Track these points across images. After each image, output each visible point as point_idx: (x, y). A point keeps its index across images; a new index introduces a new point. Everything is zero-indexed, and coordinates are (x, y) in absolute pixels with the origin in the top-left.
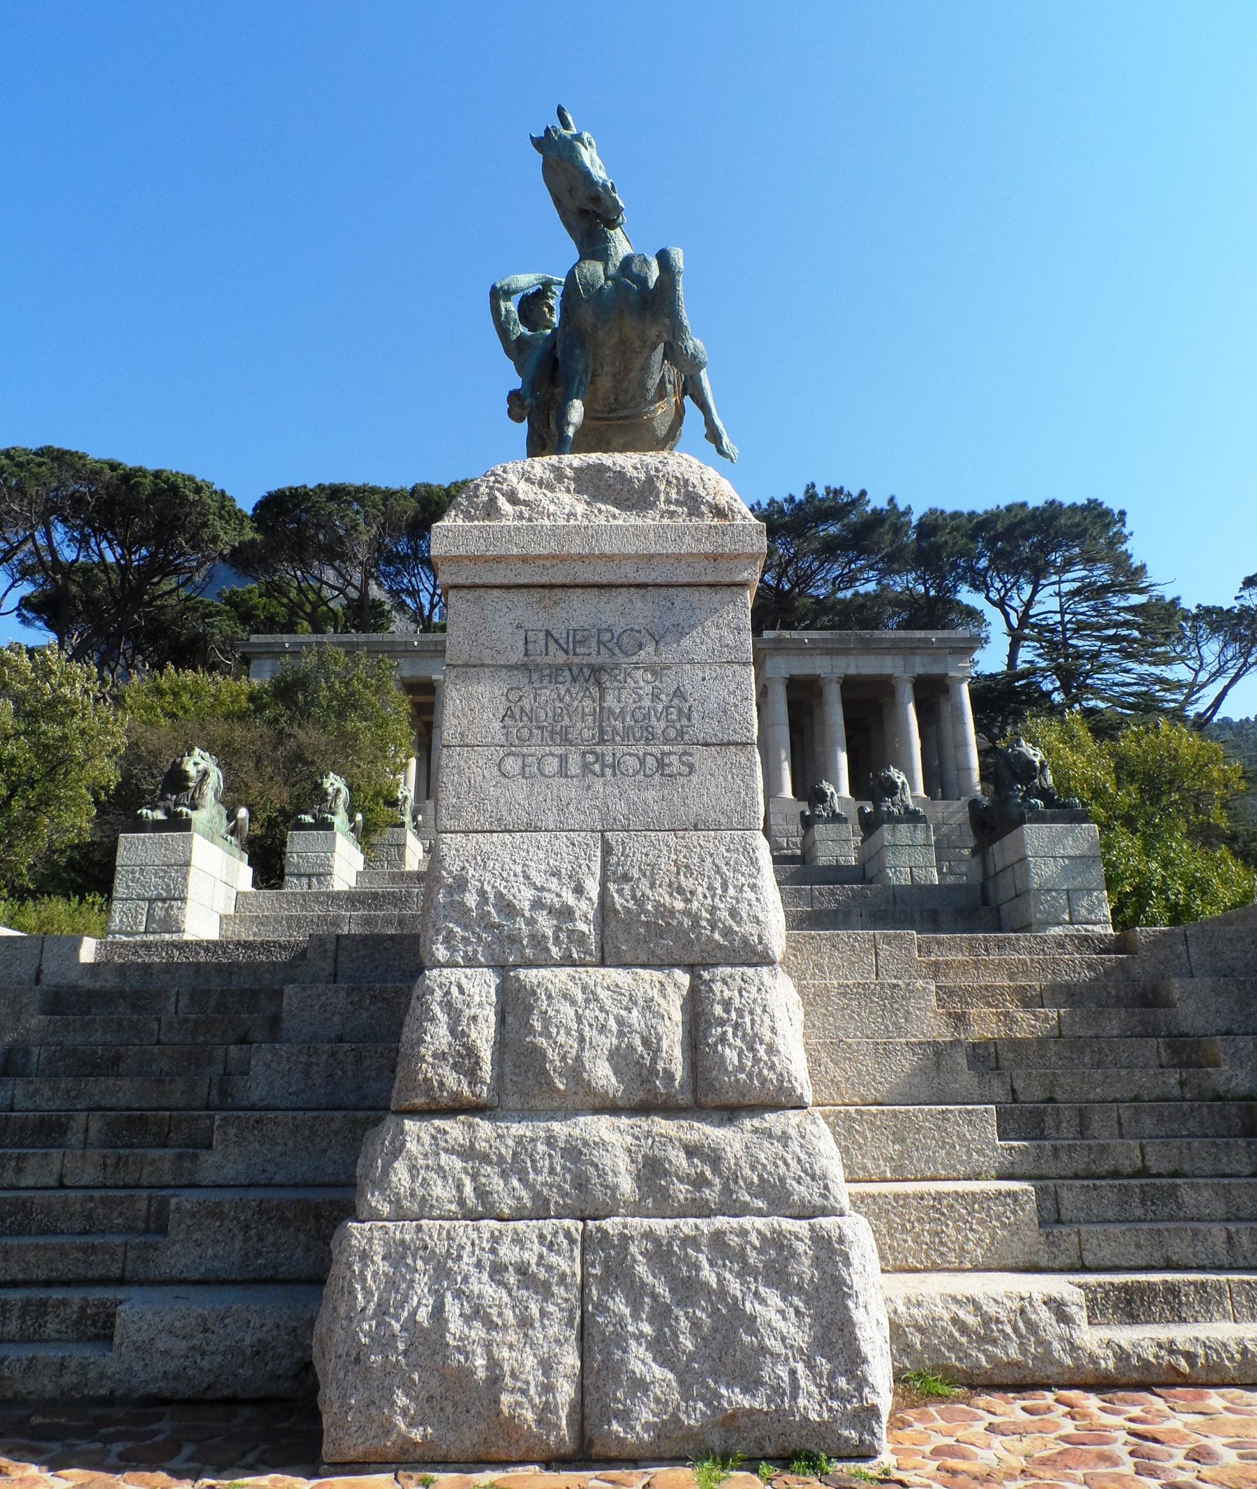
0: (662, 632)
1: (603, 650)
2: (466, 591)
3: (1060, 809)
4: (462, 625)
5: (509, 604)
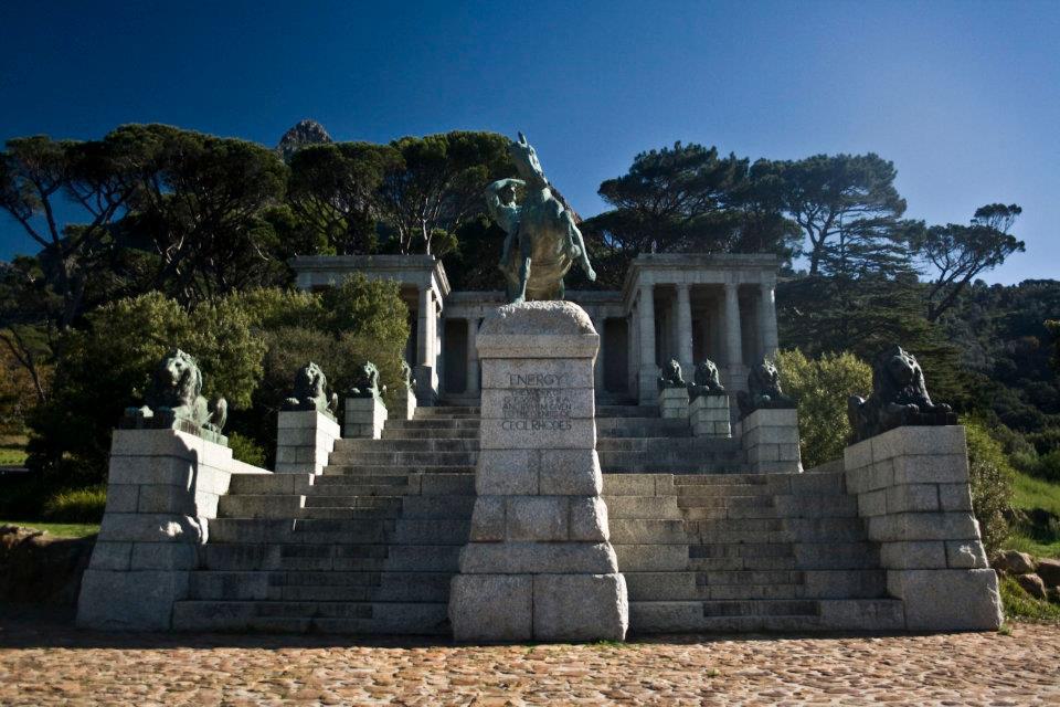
3: (778, 403)
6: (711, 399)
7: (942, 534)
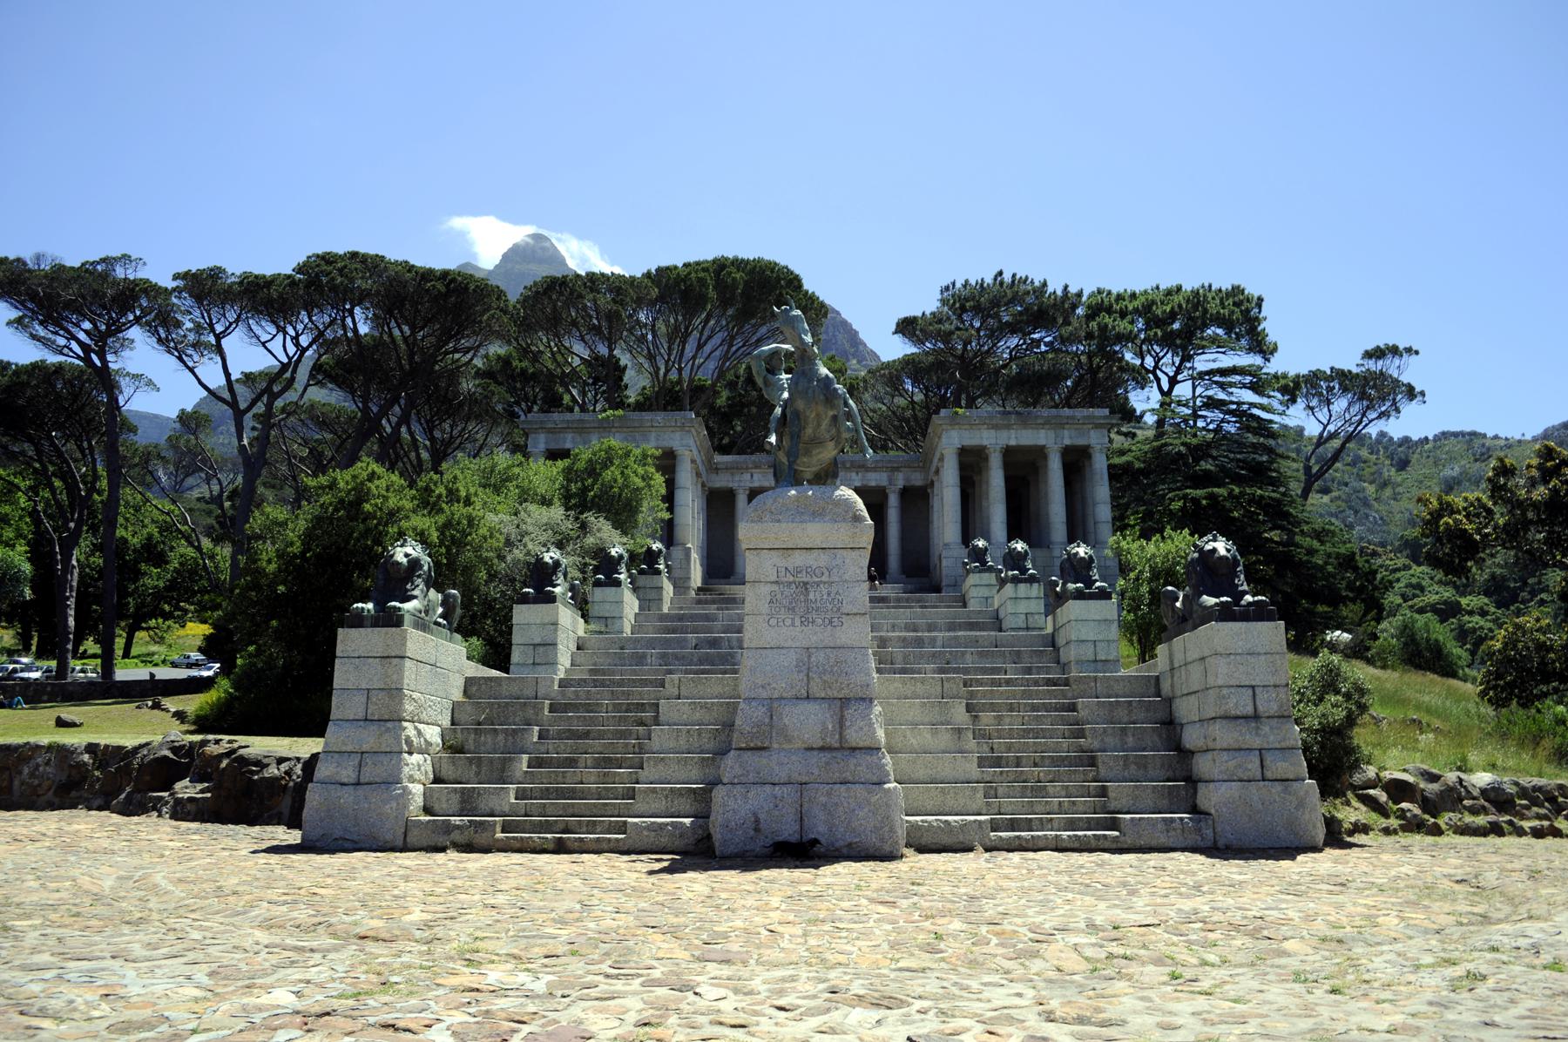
6: (1022, 586)
7: (1257, 743)
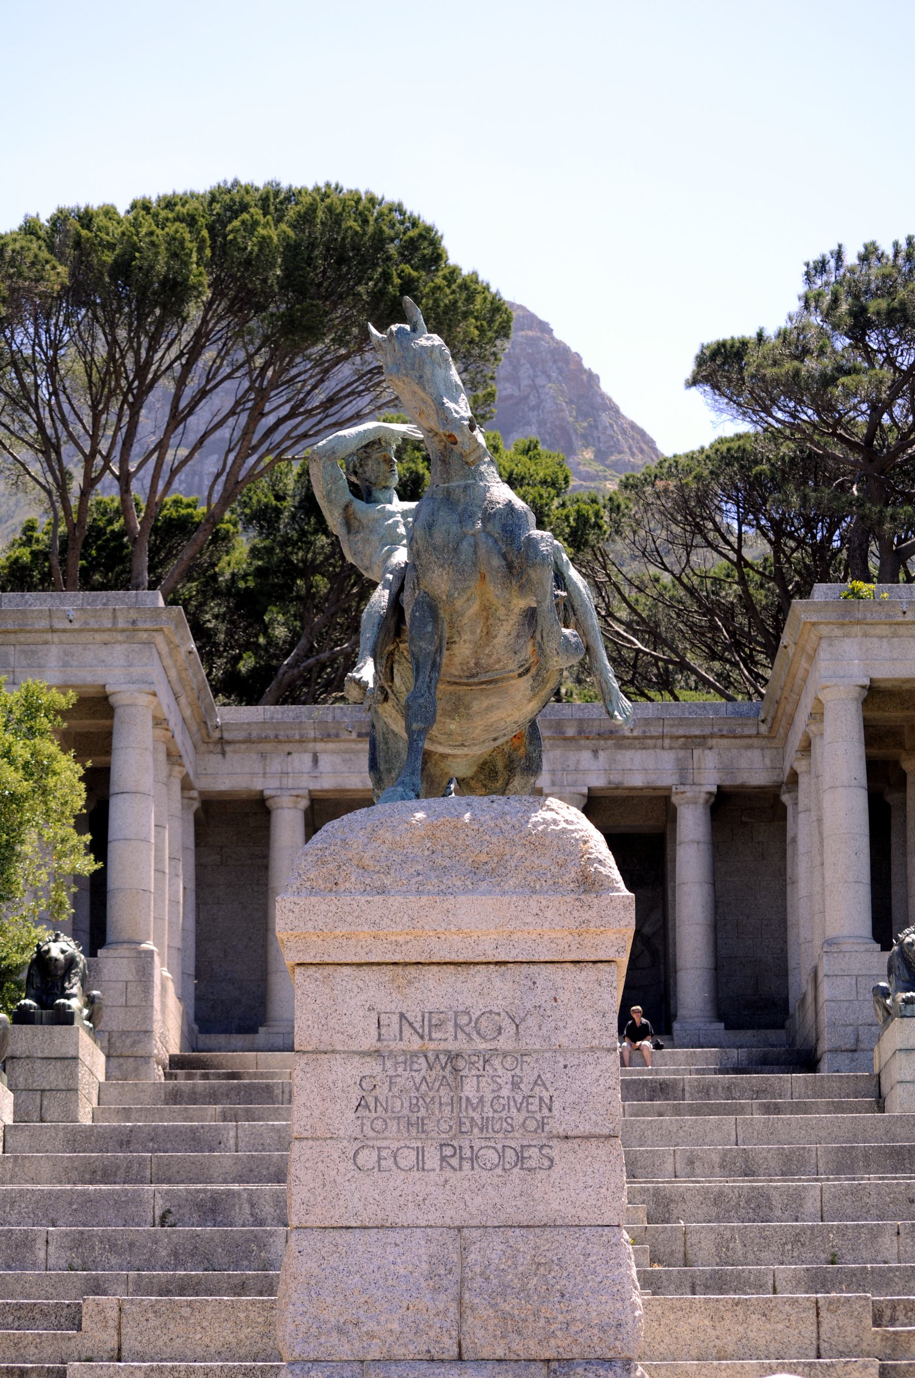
0: (522, 1015)
1: (460, 1035)
2: (314, 968)
4: (310, 1007)
5: (360, 983)
